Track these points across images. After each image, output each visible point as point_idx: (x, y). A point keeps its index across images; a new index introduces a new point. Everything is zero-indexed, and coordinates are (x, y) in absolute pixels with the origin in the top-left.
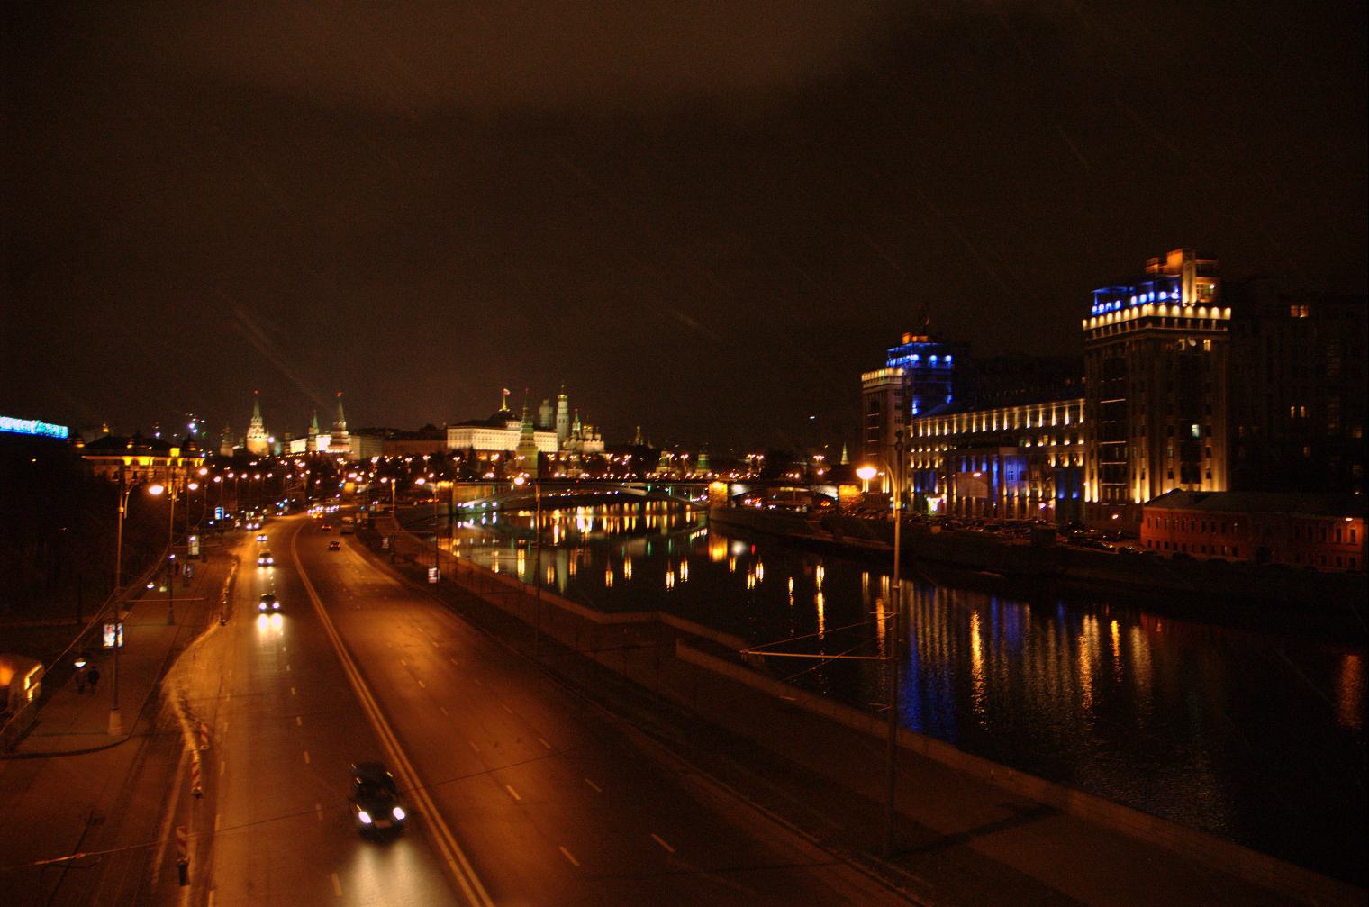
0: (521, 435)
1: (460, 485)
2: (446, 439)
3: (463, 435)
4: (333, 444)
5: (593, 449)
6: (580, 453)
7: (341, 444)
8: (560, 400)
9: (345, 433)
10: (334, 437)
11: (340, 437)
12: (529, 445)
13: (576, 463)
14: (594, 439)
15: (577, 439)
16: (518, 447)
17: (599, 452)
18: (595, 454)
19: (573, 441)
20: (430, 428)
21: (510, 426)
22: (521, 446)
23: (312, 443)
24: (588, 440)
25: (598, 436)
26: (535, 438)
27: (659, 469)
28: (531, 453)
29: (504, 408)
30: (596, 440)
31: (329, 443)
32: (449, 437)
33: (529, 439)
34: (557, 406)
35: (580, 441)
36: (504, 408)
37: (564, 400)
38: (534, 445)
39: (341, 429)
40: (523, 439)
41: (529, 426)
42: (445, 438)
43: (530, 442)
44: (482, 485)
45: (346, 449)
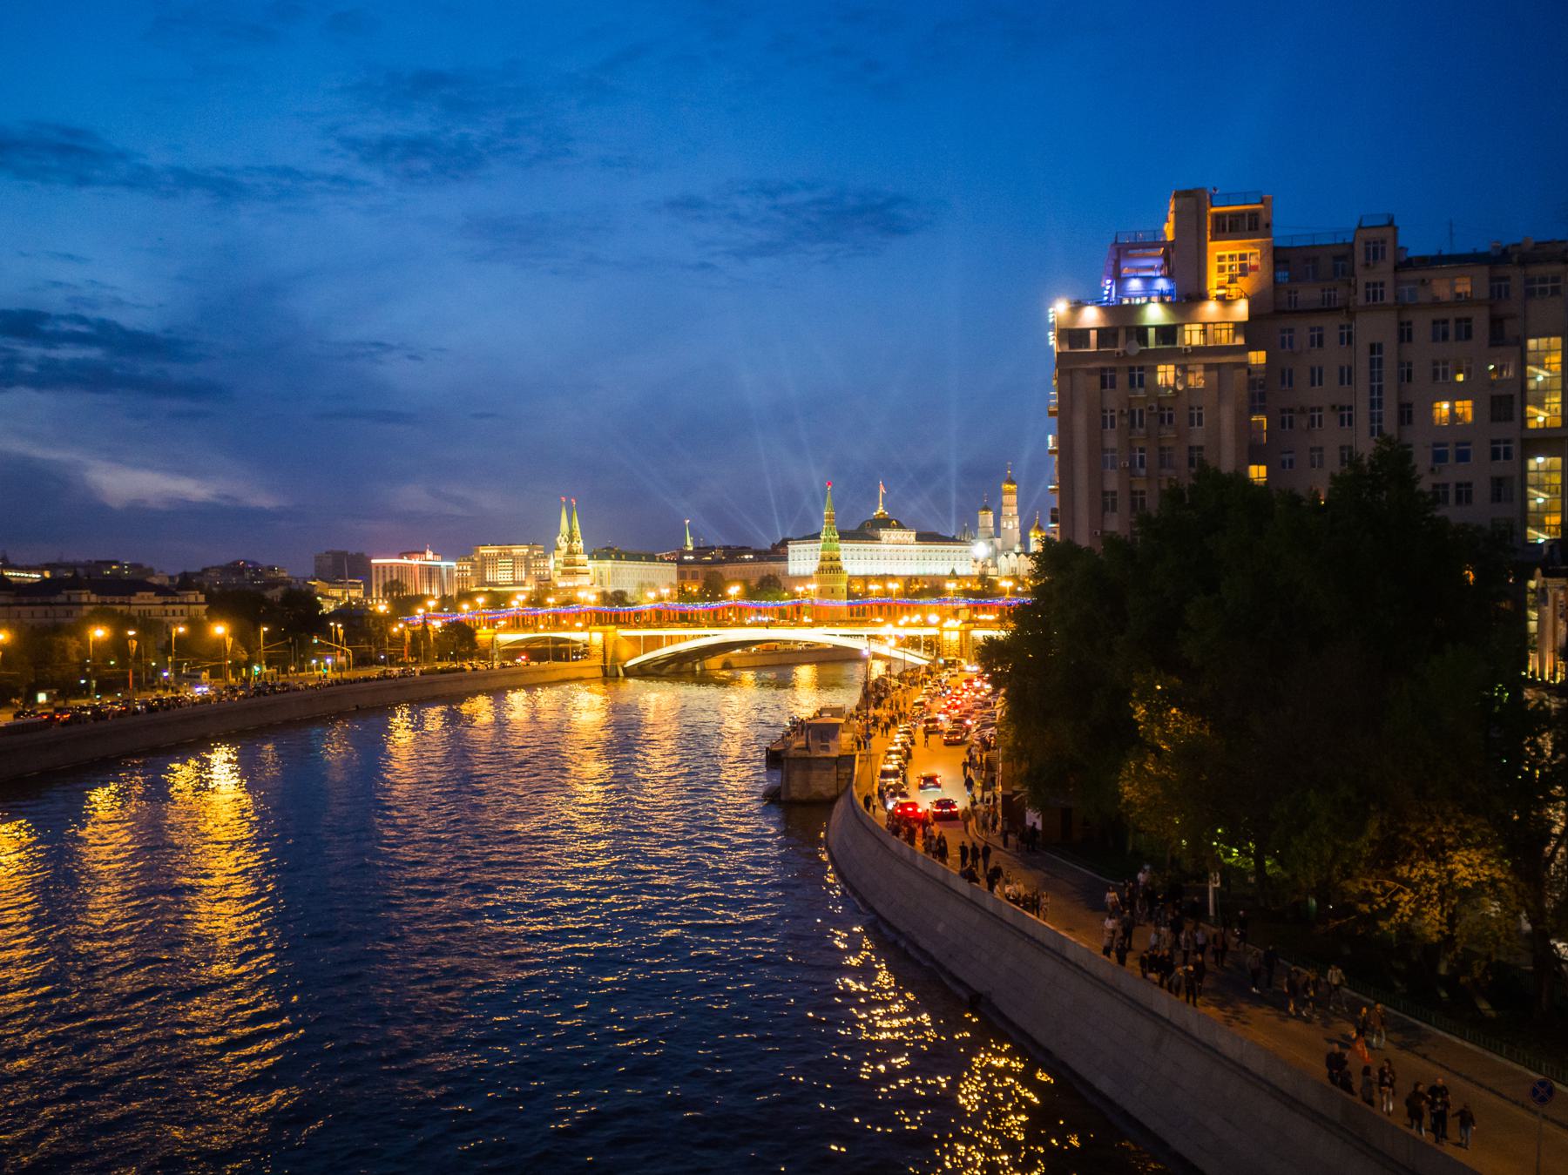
0: (820, 553)
2: (787, 560)
3: (808, 553)
12: (832, 568)
15: (1018, 554)
19: (1012, 556)
22: (821, 569)
26: (842, 555)
29: (881, 510)
32: (790, 558)
33: (831, 559)
35: (1022, 555)
36: (881, 510)
37: (1011, 492)
38: (840, 568)
40: (823, 560)
42: (784, 558)
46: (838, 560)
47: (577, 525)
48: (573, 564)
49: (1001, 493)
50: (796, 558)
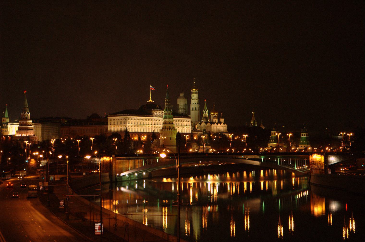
0: (163, 120)
1: (118, 159)
2: (107, 124)
4: (20, 130)
5: (219, 130)
6: (209, 133)
7: (27, 130)
8: (193, 93)
9: (30, 121)
10: (20, 125)
11: (26, 124)
12: (170, 128)
13: (206, 141)
14: (219, 122)
15: (206, 123)
16: (160, 130)
17: (223, 132)
18: (220, 134)
19: (203, 124)
20: (95, 116)
21: (155, 113)
22: (164, 128)
23: (4, 129)
24: (214, 123)
25: (222, 120)
27: (269, 145)
28: (172, 134)
29: (151, 100)
30: (221, 123)
31: (18, 130)
32: (109, 123)
33: (169, 123)
34: (191, 98)
35: (209, 124)
36: (151, 100)
37: (196, 93)
38: (174, 128)
39: (27, 119)
40: (165, 123)
41: (169, 114)
43: (170, 125)
44: (134, 159)
45: (31, 133)
46: (173, 123)
47: (27, 104)
48: (25, 125)
49: (191, 93)
50: (112, 123)
